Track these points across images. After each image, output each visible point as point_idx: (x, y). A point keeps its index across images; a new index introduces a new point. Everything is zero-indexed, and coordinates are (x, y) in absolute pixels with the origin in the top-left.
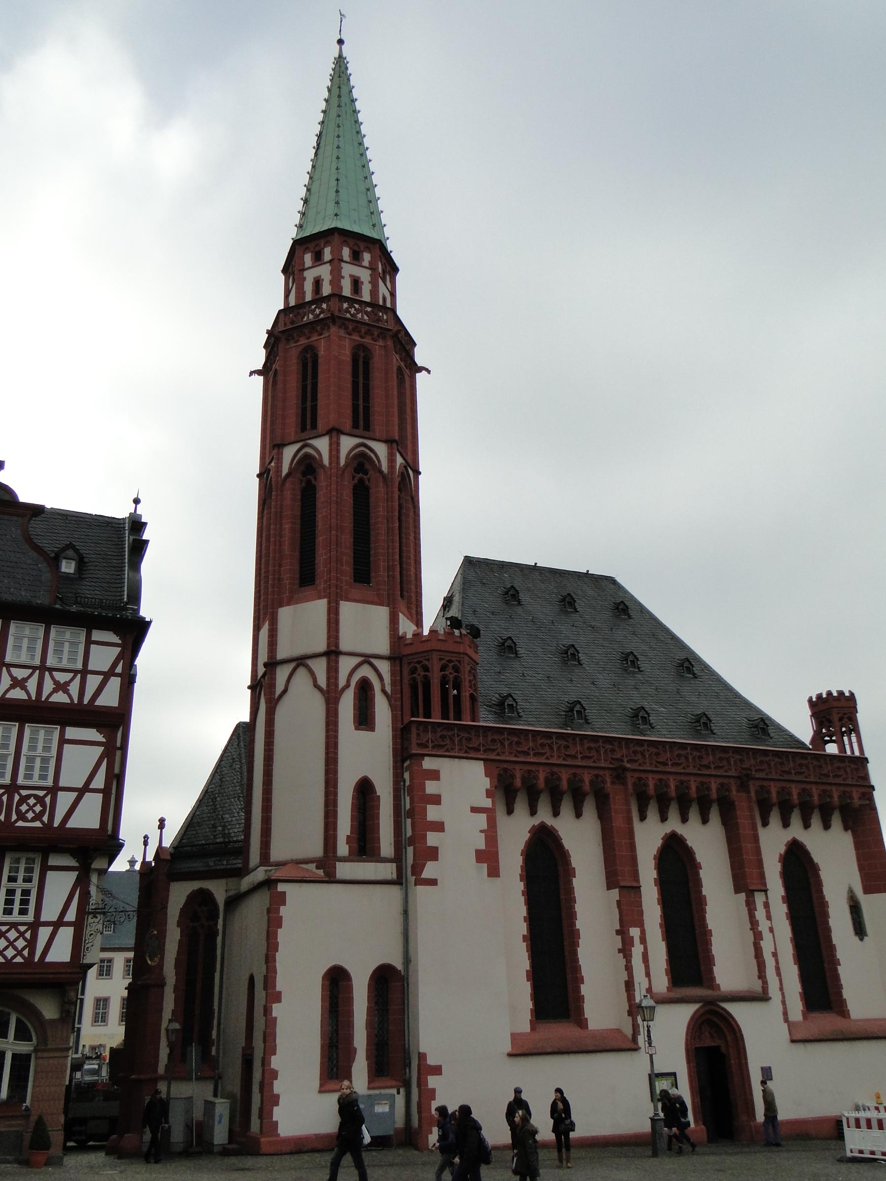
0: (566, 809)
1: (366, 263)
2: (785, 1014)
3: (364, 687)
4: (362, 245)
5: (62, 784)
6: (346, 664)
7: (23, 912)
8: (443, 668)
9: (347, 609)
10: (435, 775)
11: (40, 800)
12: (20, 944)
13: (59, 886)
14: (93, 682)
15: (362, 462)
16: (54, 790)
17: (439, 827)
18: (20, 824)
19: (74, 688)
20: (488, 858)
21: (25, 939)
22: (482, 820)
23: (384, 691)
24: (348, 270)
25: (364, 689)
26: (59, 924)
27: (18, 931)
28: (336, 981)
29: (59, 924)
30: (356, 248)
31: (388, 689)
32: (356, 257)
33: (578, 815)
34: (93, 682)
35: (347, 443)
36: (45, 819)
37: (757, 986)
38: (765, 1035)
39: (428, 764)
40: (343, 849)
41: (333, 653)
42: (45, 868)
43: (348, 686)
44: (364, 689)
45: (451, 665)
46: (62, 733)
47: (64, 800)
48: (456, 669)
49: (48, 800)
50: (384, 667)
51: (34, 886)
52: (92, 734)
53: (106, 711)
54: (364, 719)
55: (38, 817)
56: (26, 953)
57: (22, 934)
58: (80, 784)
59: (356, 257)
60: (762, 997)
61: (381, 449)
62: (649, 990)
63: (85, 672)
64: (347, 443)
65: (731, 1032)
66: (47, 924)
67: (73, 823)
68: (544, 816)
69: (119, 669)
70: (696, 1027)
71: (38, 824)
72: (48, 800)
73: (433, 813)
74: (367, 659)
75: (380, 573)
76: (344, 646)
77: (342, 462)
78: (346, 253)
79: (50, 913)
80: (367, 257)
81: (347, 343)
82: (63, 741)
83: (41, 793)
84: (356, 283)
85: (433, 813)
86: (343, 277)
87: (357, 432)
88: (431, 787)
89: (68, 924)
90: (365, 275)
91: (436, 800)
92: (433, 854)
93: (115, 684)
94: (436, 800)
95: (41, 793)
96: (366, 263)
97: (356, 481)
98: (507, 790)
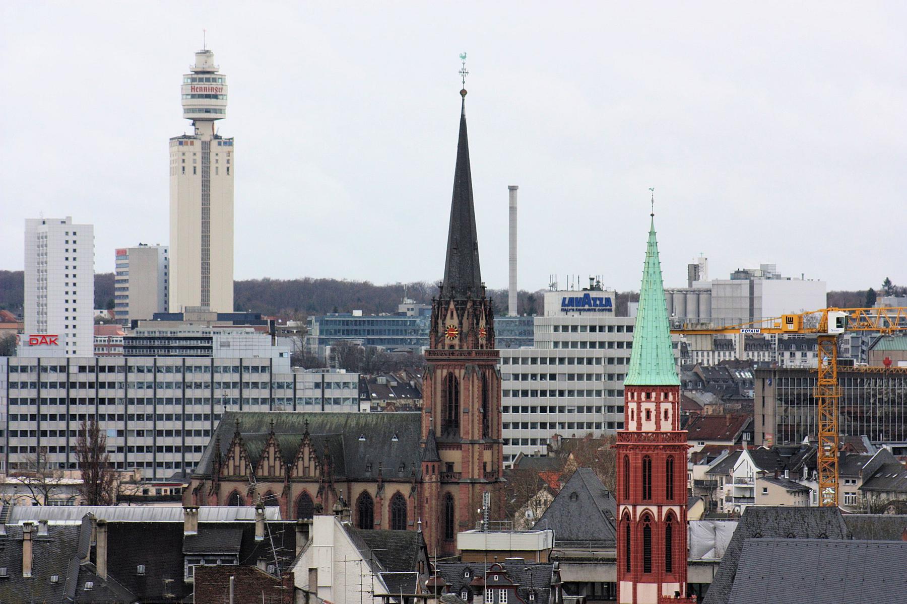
1: (653, 399)
4: (651, 389)
9: (640, 586)
15: (647, 516)
24: (645, 406)
32: (648, 396)
35: (640, 509)
59: (648, 396)
61: (654, 509)
64: (640, 509)
75: (654, 569)
77: (638, 519)
78: (643, 395)
80: (654, 395)
81: (640, 457)
84: (648, 412)
90: (652, 406)
96: (653, 399)
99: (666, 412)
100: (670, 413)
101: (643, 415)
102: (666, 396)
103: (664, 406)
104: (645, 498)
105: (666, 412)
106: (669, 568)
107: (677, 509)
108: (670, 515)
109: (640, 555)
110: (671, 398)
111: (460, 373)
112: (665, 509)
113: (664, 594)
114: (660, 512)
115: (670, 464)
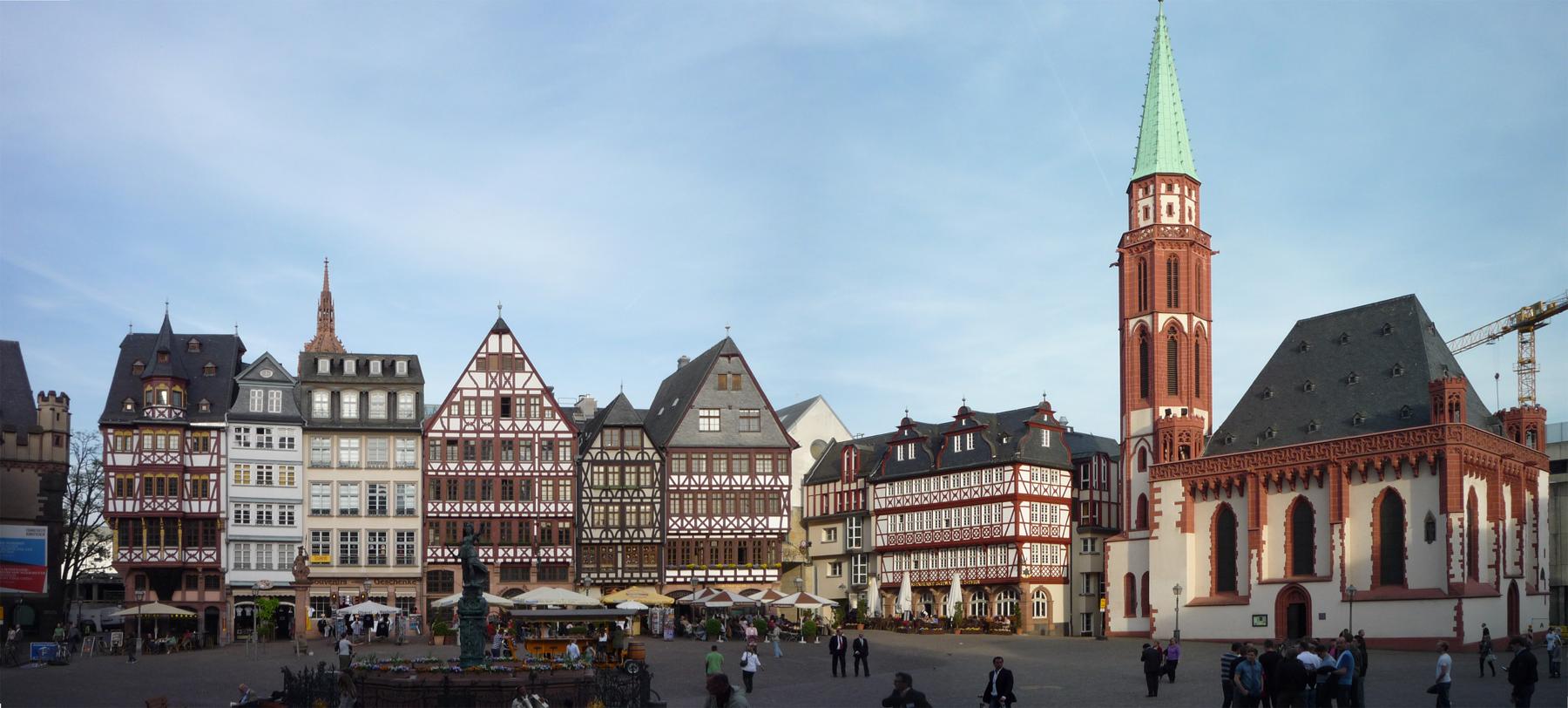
0: (1235, 494)
2: (1343, 588)
6: (1133, 442)
10: (1159, 490)
13: (1012, 553)
15: (1143, 330)
17: (1160, 514)
20: (1184, 525)
22: (1180, 507)
24: (1142, 204)
28: (1130, 578)
32: (1146, 190)
33: (1242, 495)
37: (1327, 573)
38: (1323, 597)
39: (1156, 485)
40: (1134, 526)
44: (1143, 451)
50: (1150, 439)
54: (1142, 466)
59: (1146, 190)
60: (1328, 579)
61: (1147, 319)
62: (1259, 578)
64: (1132, 323)
65: (1305, 596)
68: (1223, 499)
70: (1281, 595)
73: (1157, 508)
74: (1142, 437)
76: (1133, 431)
84: (1146, 209)
85: (1157, 508)
88: (1157, 496)
91: (1159, 501)
92: (1157, 526)
94: (1159, 501)
98: (1195, 492)
99: (1170, 207)
100: (1176, 208)
102: (1170, 188)
105: (1170, 207)
106: (1174, 389)
107: (1183, 319)
108: (1174, 327)
109: (1137, 376)
110: (1177, 189)
111: (1403, 487)
112: (1163, 319)
115: (1173, 266)
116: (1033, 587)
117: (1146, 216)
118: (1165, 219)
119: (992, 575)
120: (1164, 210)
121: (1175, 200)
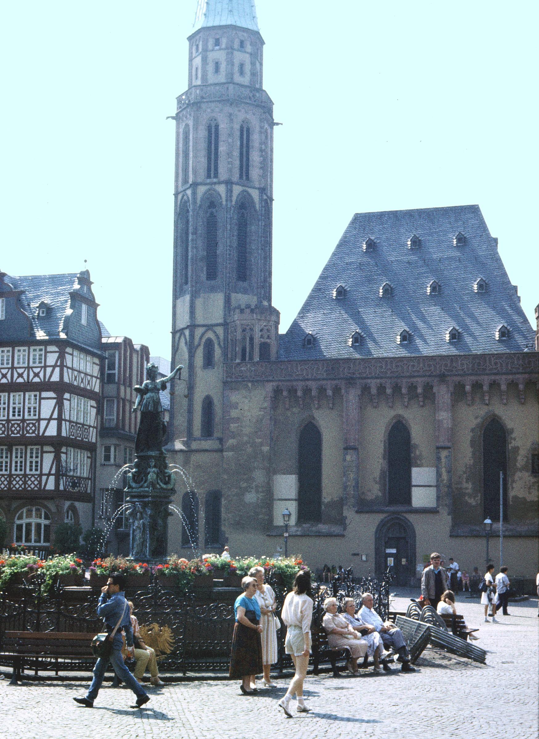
3: (209, 343)
5: (42, 417)
6: (199, 332)
7: (36, 470)
8: (244, 330)
11: (34, 425)
12: (36, 483)
13: (48, 459)
14: (49, 370)
16: (39, 420)
18: (28, 435)
19: (41, 375)
21: (37, 481)
23: (219, 344)
25: (209, 344)
26: (49, 474)
27: (35, 478)
29: (49, 474)
30: (218, 37)
31: (222, 344)
32: (217, 42)
34: (49, 370)
36: (36, 432)
41: (192, 327)
42: (43, 452)
43: (199, 345)
44: (209, 344)
45: (248, 328)
46: (40, 395)
47: (43, 424)
48: (251, 329)
49: (37, 424)
50: (220, 331)
51: (39, 460)
52: (51, 394)
53: (55, 383)
54: (209, 362)
55: (34, 432)
56: (38, 486)
57: (36, 479)
58: (48, 417)
63: (45, 367)
66: (45, 475)
67: (47, 434)
69: (59, 364)
71: (34, 435)
72: (37, 424)
74: (209, 327)
79: (46, 470)
82: (41, 398)
83: (34, 422)
86: (207, 64)
87: (208, 181)
89: (52, 475)
93: (57, 370)
95: (34, 422)
97: (208, 215)
101: (211, 68)
102: (242, 44)
103: (239, 56)
104: (209, 176)
105: (242, 66)
107: (255, 194)
110: (249, 48)
112: (237, 190)
113: (234, 303)
114: (230, 192)
115: (245, 133)
116: (67, 504)
117: (217, 69)
118: (237, 78)
119: (17, 484)
120: (236, 69)
121: (247, 59)
